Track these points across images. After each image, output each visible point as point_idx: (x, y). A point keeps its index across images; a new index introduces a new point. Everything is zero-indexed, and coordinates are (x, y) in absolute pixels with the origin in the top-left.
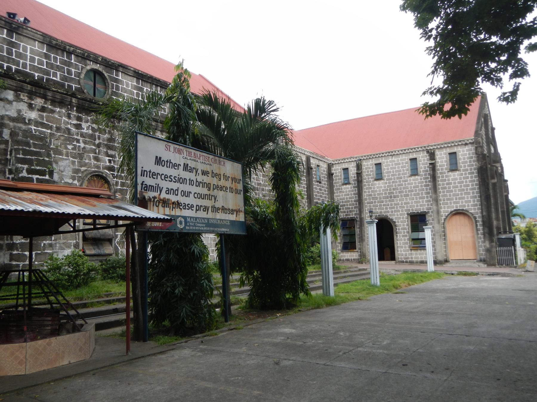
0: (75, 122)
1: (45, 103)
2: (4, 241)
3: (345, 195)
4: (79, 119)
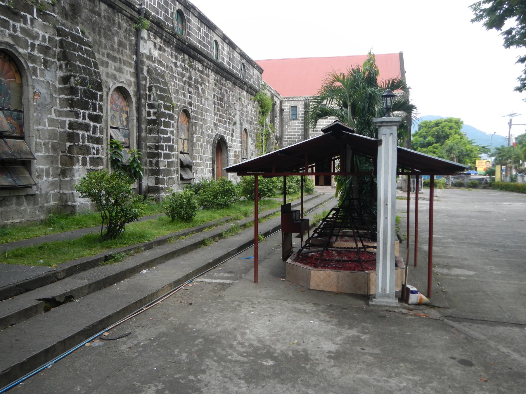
0: (174, 61)
1: (161, 43)
2: (147, 167)
3: (292, 129)
4: (176, 58)
